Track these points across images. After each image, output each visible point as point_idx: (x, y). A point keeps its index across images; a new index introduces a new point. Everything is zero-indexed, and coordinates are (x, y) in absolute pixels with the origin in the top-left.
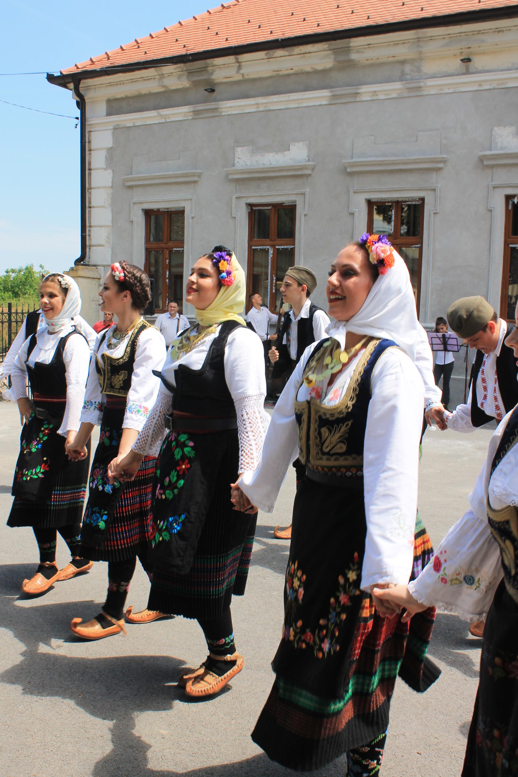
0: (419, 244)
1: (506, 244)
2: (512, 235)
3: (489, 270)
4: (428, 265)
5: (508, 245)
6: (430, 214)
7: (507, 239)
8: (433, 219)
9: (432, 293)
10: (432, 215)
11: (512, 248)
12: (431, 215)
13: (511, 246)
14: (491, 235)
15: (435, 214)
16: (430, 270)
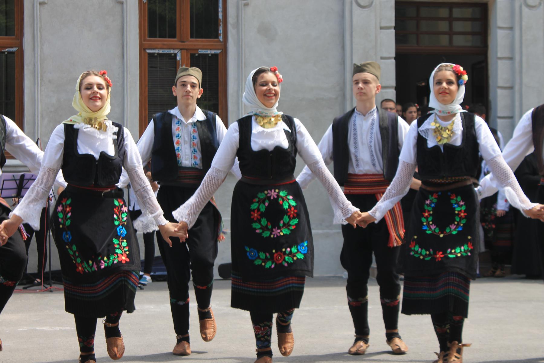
0: (16, 47)
1: (142, 48)
2: (148, 37)
3: (123, 84)
4: (34, 76)
5: (145, 49)
6: (33, 5)
7: (143, 42)
8: (38, 11)
9: (42, 116)
10: (37, 6)
11: (149, 54)
12: (35, 5)
13: (148, 51)
14: (123, 35)
15: (41, 4)
16: (38, 84)
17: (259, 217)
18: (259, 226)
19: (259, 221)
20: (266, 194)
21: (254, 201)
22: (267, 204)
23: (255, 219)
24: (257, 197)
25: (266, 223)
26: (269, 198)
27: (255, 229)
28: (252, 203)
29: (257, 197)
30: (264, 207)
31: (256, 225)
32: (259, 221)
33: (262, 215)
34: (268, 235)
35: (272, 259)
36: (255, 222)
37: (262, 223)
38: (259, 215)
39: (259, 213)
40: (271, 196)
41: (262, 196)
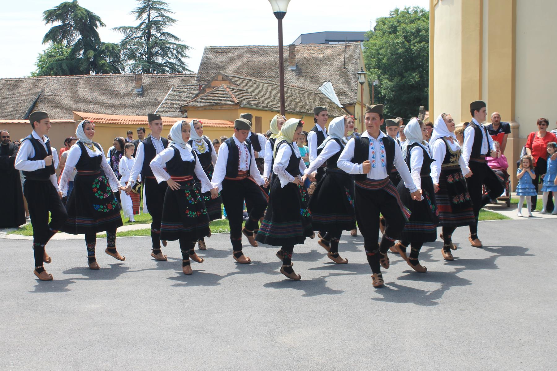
17: (97, 191)
18: (98, 195)
19: (97, 192)
20: (98, 180)
21: (93, 184)
22: (99, 184)
23: (95, 192)
24: (94, 182)
25: (100, 192)
26: (99, 181)
27: (97, 196)
28: (93, 185)
29: (94, 182)
30: (99, 185)
31: (96, 195)
32: (97, 192)
33: (98, 189)
34: (102, 198)
35: (107, 208)
36: (96, 193)
37: (99, 193)
38: (97, 190)
39: (97, 189)
40: (100, 180)
41: (96, 181)
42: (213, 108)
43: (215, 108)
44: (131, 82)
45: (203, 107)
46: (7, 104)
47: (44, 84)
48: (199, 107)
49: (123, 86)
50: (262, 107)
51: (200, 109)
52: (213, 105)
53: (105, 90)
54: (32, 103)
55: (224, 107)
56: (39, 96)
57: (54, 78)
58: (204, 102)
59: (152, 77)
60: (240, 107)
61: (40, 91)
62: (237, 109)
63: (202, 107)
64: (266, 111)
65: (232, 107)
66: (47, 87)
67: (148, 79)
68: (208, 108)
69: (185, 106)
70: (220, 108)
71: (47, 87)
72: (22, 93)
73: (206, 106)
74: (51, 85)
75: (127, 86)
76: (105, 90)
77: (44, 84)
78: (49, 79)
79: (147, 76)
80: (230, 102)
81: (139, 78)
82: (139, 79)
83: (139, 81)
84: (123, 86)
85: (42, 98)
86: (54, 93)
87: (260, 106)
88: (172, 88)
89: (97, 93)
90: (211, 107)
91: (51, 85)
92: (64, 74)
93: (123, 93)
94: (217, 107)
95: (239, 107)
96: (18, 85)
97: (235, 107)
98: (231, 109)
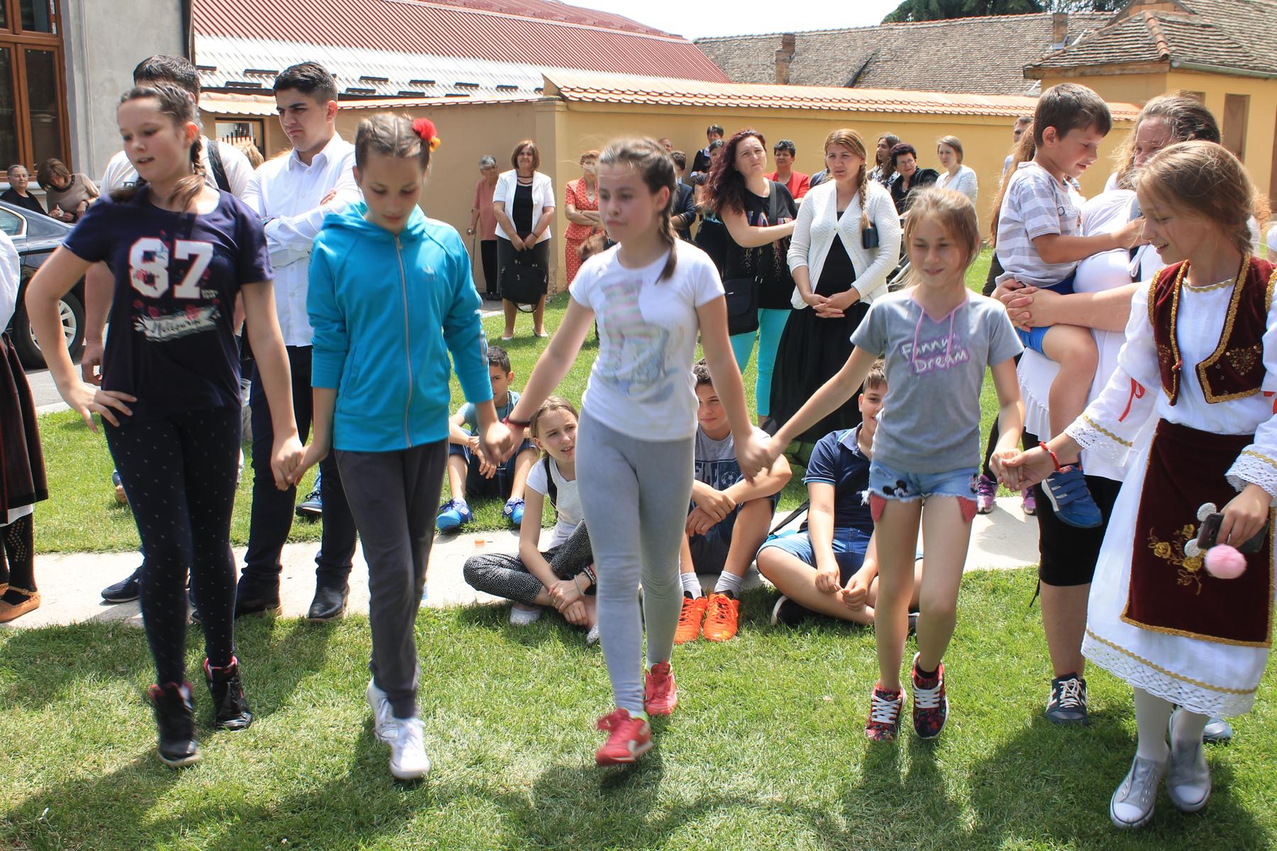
42: (1102, 70)
43: (1106, 70)
44: (1046, 31)
45: (1077, 70)
46: (808, 78)
47: (881, 40)
48: (1066, 70)
49: (1029, 38)
50: (1250, 68)
51: (1071, 74)
52: (1103, 64)
53: (991, 48)
54: (851, 77)
55: (1130, 67)
56: (867, 63)
57: (901, 27)
58: (1083, 56)
59: (1090, 19)
60: (1171, 66)
61: (871, 52)
62: (1162, 74)
63: (1075, 68)
64: (1266, 79)
65: (1149, 67)
66: (885, 45)
67: (1082, 22)
68: (1088, 71)
69: (1035, 66)
70: (1118, 72)
71: (885, 45)
72: (840, 56)
73: (1084, 66)
74: (893, 41)
75: (1036, 39)
76: (991, 48)
77: (881, 40)
78: (892, 29)
79: (1082, 17)
80: (1147, 56)
81: (1061, 20)
82: (1062, 22)
83: (1061, 28)
84: (1029, 38)
85: (871, 67)
86: (896, 56)
87: (1240, 66)
88: (1082, 34)
89: (976, 54)
90: (1097, 69)
91: (893, 41)
92: (933, 17)
93: (1026, 53)
94: (1113, 68)
95: (1167, 68)
96: (837, 41)
97: (1158, 68)
98: (1148, 74)
